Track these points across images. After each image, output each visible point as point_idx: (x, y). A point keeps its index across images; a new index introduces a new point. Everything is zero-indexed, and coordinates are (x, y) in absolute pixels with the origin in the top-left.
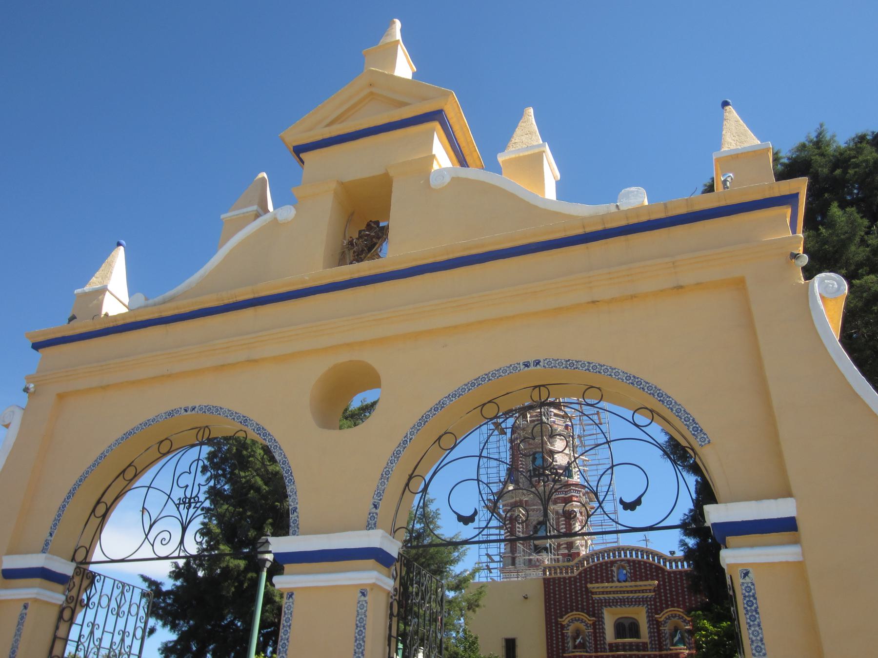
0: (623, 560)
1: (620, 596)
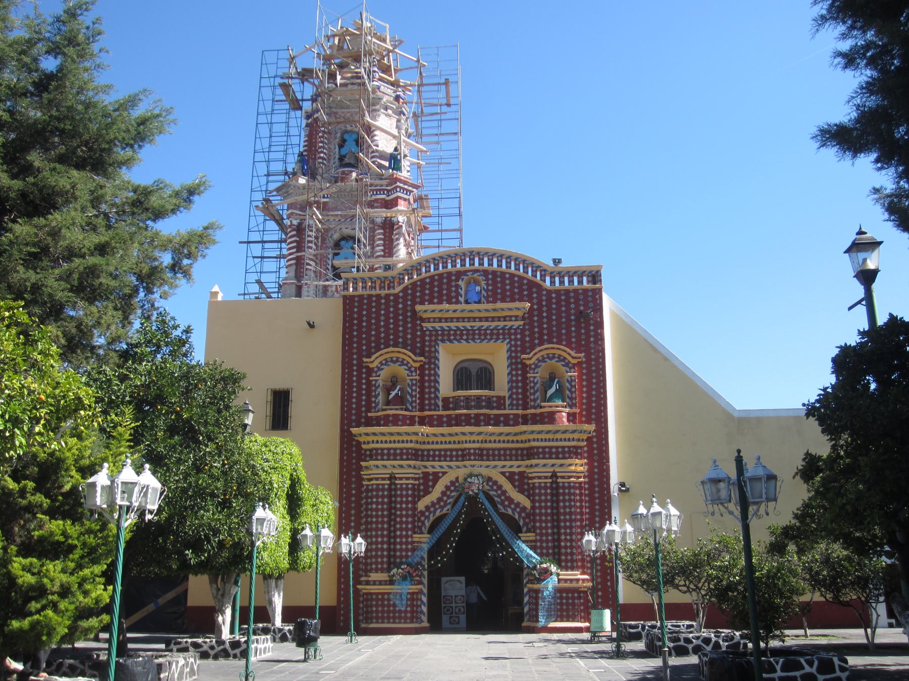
0: (476, 271)
1: (468, 325)
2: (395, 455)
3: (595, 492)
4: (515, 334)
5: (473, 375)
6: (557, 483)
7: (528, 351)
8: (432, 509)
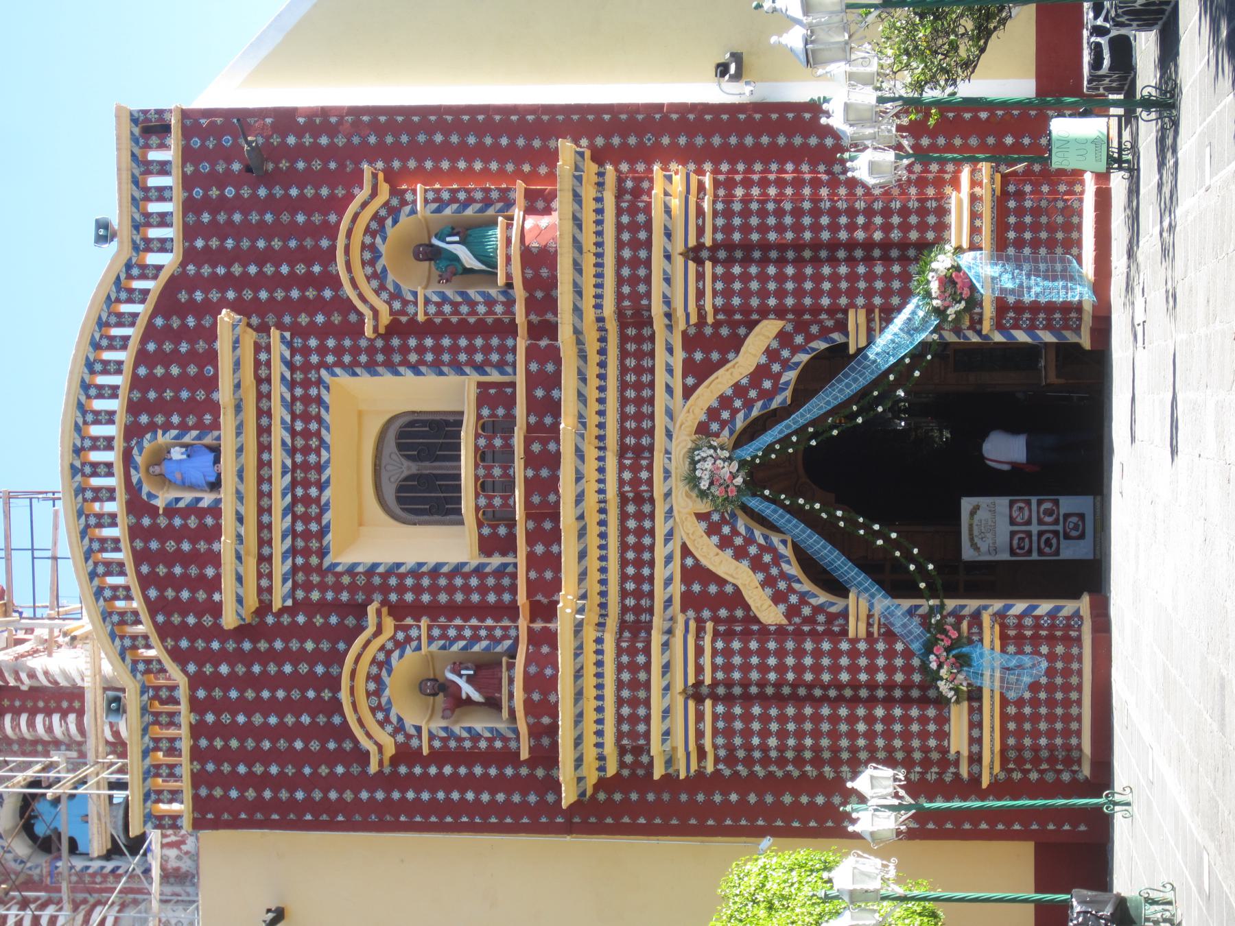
1: (280, 483)
2: (634, 685)
3: (741, 145)
4: (306, 351)
5: (420, 469)
6: (715, 247)
7: (353, 318)
8: (782, 585)
